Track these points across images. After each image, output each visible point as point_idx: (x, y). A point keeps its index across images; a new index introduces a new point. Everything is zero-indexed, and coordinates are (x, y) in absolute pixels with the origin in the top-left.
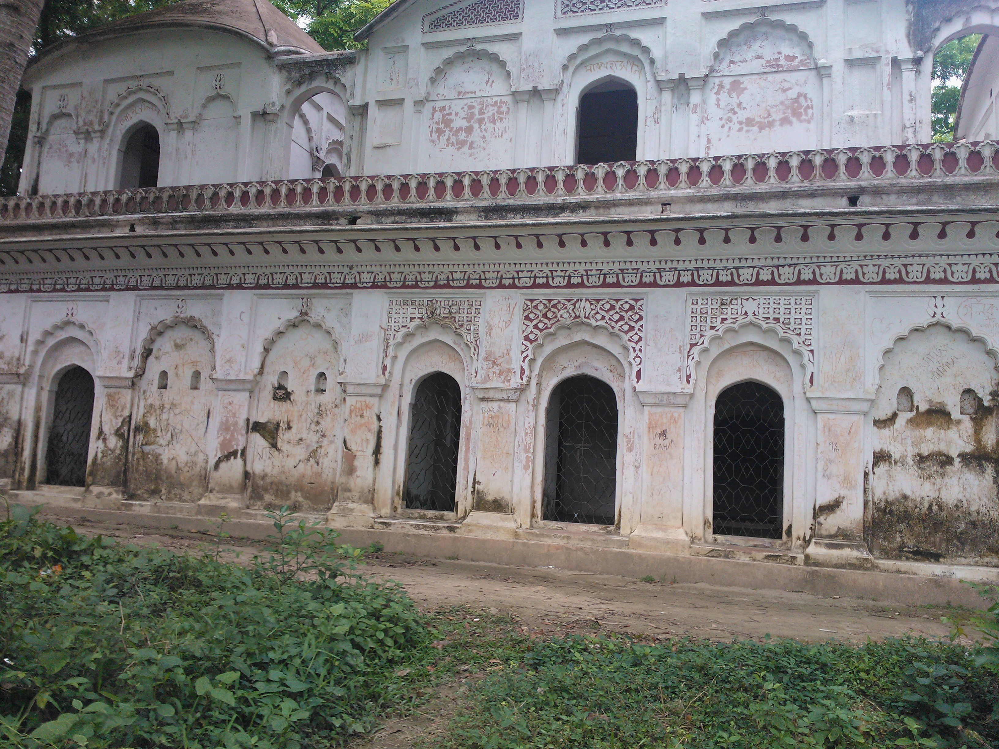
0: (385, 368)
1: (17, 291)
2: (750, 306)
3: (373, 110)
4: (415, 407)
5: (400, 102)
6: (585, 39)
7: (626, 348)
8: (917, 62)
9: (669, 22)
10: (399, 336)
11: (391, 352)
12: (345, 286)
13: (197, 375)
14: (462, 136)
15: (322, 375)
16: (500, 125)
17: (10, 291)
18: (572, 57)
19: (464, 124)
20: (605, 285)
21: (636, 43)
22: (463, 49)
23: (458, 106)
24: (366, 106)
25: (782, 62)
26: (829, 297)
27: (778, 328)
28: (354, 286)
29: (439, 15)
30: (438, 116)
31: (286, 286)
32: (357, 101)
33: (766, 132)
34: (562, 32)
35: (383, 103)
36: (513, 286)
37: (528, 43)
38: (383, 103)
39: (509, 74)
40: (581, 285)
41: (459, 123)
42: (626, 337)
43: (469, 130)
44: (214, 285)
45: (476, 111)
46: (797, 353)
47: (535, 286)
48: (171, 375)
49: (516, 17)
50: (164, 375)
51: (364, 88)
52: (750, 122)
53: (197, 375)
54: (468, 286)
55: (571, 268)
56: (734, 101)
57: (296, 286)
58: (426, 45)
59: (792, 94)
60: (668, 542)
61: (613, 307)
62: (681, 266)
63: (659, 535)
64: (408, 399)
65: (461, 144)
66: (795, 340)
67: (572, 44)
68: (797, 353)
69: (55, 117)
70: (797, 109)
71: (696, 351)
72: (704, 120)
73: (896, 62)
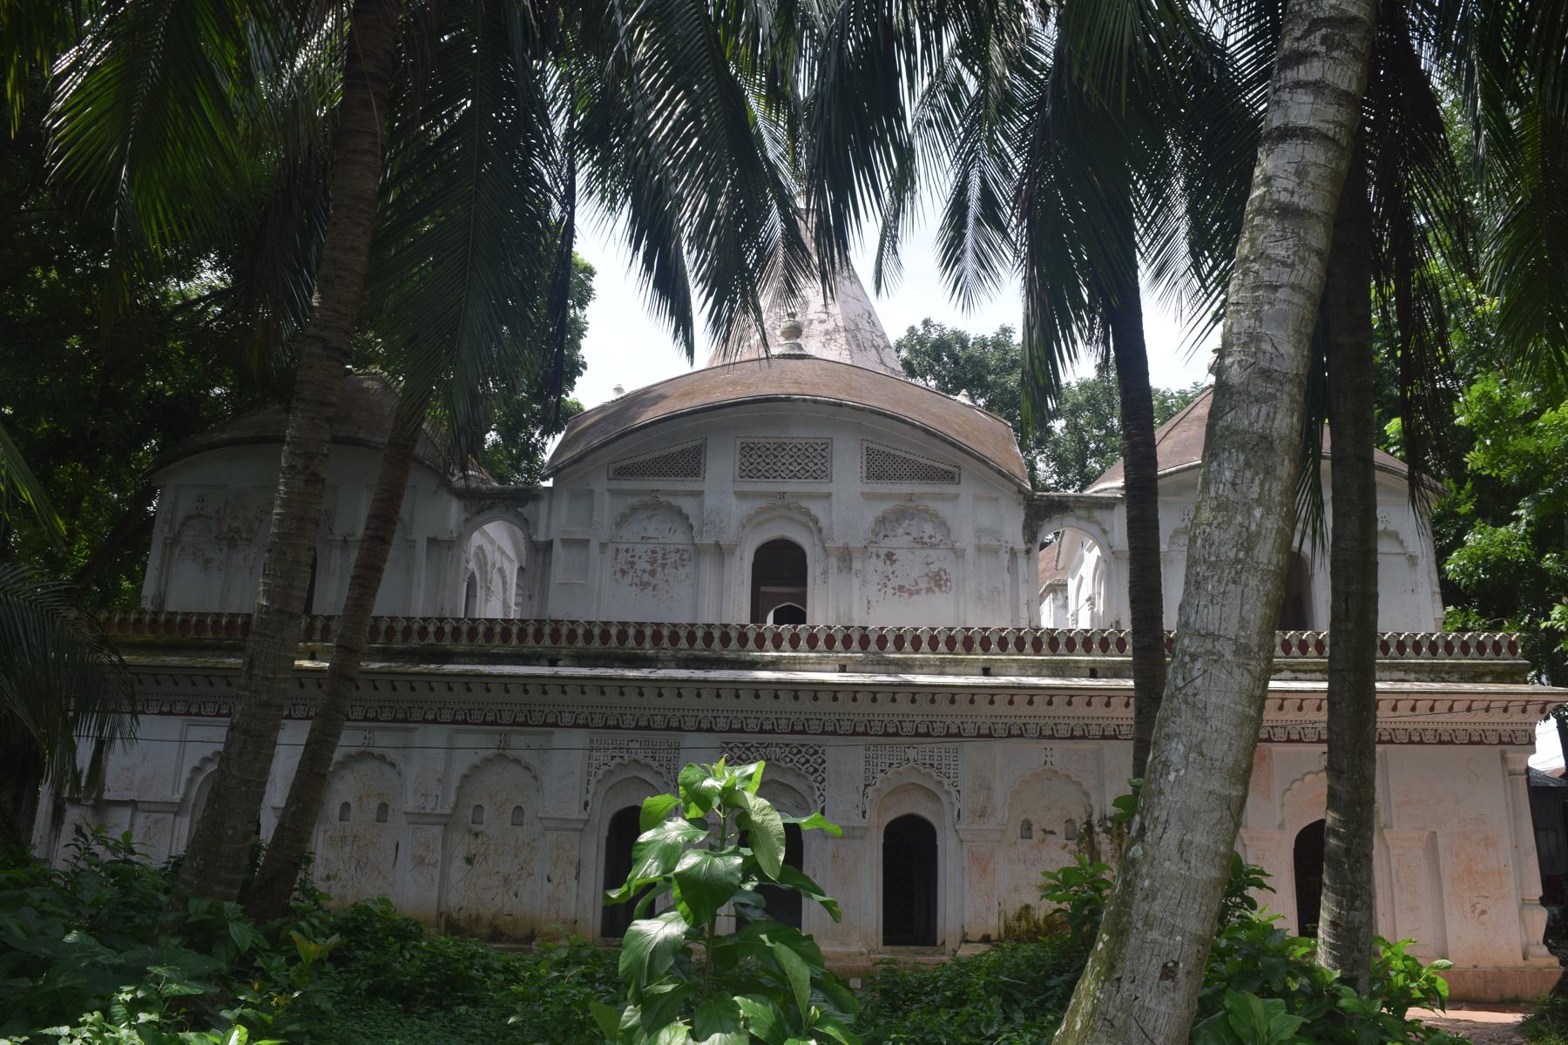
0: (586, 804)
1: (170, 713)
2: (912, 754)
3: (558, 549)
4: (608, 839)
5: (586, 542)
6: (762, 503)
7: (811, 787)
8: (1028, 552)
9: (834, 497)
10: (600, 772)
11: (592, 787)
12: (545, 725)
13: (383, 808)
14: (646, 577)
15: (519, 808)
16: (682, 571)
17: (161, 713)
18: (750, 518)
19: (648, 567)
20: (793, 732)
21: (808, 513)
22: (648, 499)
23: (640, 549)
24: (550, 544)
25: (926, 539)
26: (971, 750)
27: (933, 772)
28: (556, 725)
29: (624, 463)
30: (622, 557)
31: (485, 723)
32: (541, 537)
33: (915, 598)
34: (741, 495)
35: (568, 543)
36: (710, 730)
37: (710, 502)
38: (568, 543)
39: (691, 527)
40: (772, 731)
41: (642, 565)
42: (812, 778)
43: (653, 573)
44: (404, 718)
45: (659, 556)
46: (948, 793)
47: (731, 730)
48: (353, 806)
49: (697, 475)
50: (346, 806)
51: (548, 526)
52: (901, 588)
53: (383, 808)
54: (669, 728)
55: (763, 716)
56: (889, 569)
57: (494, 723)
58: (613, 492)
59: (934, 568)
60: (849, 955)
61: (799, 752)
62: (856, 718)
63: (840, 949)
64: (605, 832)
65: (644, 585)
66: (946, 781)
67: (749, 507)
68: (948, 793)
69: (189, 518)
70: (938, 581)
71: (869, 790)
72: (864, 582)
73: (1013, 552)
